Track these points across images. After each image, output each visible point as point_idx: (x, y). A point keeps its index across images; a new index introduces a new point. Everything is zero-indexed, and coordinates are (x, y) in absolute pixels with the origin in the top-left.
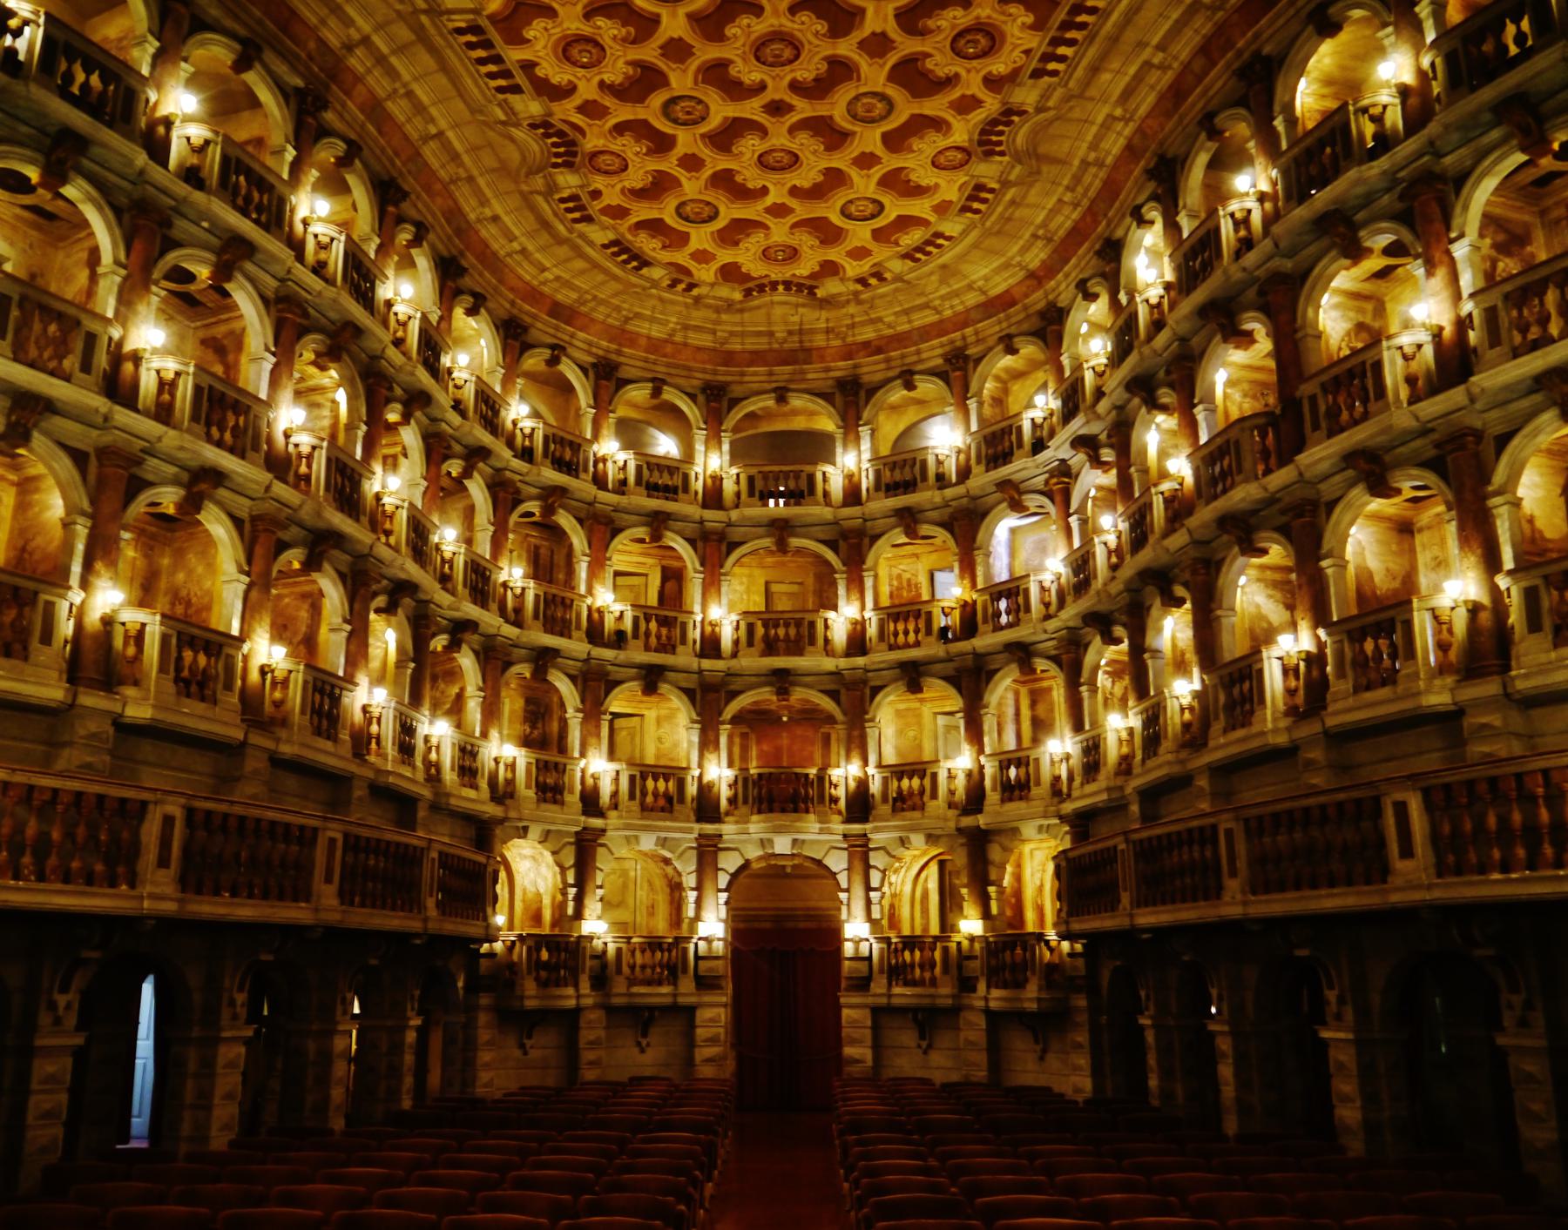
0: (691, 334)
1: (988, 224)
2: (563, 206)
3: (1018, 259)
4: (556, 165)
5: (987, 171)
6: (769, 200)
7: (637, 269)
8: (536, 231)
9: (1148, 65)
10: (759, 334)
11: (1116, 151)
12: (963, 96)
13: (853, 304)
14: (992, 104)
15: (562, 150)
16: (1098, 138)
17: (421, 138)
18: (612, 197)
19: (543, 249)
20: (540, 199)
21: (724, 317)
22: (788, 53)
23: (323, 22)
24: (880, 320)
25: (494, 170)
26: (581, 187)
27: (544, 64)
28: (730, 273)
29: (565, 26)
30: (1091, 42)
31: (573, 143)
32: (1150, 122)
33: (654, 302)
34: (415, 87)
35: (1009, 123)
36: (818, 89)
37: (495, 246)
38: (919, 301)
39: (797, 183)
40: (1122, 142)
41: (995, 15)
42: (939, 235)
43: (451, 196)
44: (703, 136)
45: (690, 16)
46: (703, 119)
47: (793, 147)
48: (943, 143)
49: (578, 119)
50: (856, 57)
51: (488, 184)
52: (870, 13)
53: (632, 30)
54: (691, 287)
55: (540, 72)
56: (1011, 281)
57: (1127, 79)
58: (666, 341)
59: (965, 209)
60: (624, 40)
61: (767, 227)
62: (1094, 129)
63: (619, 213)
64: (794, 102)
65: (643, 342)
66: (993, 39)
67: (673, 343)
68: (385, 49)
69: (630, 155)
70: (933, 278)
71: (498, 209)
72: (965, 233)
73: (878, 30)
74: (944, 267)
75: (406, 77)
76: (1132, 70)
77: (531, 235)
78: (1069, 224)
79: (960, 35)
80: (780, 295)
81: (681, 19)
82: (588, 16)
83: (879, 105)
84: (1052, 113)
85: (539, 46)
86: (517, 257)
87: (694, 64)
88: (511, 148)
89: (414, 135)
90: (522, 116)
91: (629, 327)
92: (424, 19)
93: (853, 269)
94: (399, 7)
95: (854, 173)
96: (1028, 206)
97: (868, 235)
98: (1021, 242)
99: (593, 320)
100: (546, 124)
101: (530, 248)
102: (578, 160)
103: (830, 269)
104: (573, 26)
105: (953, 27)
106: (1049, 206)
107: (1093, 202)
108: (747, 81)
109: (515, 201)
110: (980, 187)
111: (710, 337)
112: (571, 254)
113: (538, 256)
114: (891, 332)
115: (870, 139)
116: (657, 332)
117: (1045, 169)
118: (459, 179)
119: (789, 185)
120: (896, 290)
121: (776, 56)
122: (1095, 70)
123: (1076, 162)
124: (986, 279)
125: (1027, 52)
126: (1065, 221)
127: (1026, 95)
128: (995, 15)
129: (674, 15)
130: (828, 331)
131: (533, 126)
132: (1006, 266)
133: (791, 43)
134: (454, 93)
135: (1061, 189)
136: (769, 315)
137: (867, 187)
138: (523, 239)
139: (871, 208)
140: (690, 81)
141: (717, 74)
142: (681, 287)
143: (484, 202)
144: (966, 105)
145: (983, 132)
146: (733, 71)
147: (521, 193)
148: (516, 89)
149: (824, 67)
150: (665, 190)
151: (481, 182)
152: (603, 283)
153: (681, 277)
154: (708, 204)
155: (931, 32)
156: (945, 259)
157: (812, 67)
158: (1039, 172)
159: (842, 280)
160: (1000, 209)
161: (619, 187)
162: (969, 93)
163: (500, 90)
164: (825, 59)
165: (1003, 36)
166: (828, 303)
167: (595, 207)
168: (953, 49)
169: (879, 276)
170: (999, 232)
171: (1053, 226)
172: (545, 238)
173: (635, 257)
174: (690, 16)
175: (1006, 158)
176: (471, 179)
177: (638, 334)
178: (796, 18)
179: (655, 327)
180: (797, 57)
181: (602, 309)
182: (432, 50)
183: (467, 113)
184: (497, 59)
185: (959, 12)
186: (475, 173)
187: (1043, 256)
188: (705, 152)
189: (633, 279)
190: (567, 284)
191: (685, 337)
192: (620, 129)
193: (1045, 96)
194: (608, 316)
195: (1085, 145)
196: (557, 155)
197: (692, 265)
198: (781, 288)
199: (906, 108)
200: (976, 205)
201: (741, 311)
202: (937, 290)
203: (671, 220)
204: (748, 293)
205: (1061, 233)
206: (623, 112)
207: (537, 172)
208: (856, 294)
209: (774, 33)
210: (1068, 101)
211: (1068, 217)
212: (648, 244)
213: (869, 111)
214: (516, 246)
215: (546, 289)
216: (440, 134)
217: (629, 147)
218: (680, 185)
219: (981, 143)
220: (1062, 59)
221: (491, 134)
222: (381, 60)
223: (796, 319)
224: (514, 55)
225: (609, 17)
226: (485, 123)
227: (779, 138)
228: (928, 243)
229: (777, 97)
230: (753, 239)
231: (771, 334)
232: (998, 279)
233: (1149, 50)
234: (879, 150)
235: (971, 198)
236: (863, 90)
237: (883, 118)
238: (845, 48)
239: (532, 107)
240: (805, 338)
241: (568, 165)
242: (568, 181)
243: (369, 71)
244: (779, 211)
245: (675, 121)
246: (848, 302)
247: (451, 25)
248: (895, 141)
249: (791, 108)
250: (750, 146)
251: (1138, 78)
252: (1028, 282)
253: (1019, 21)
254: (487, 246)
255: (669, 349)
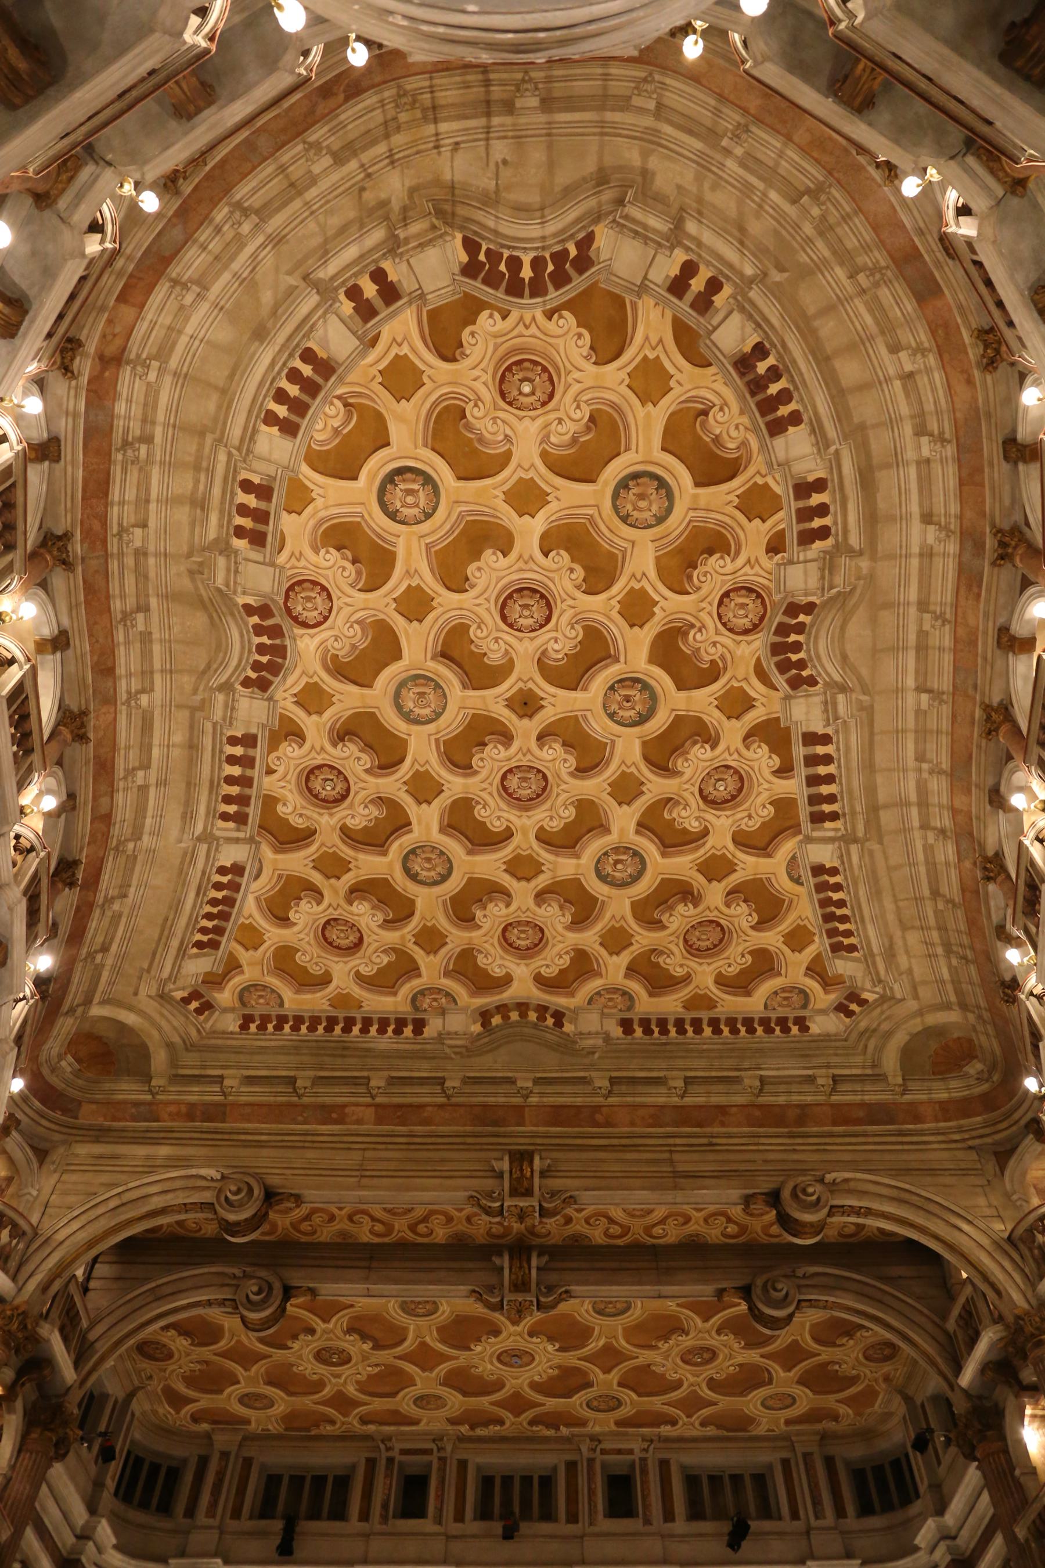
0: (706, 116)
1: (222, 457)
2: (827, 521)
3: (152, 376)
4: (809, 608)
5: (258, 579)
6: (537, 525)
7: (760, 351)
8: (888, 466)
9: (146, 766)
10: (571, 103)
11: (121, 652)
12: (320, 713)
13: (396, 206)
14: (286, 690)
15: (793, 638)
16: (146, 655)
17: (941, 701)
18: (755, 534)
19: (892, 422)
20: (854, 541)
21: (632, 155)
22: (513, 782)
23: (947, 864)
24: (339, 159)
25: (888, 606)
26: (791, 562)
27: (767, 773)
28: (610, 336)
29: (730, 820)
30: (212, 782)
31: (776, 649)
32: (110, 717)
33: (755, 228)
34: (911, 763)
35: (257, 666)
36: (482, 731)
37: (952, 470)
38: (277, 222)
39: (503, 562)
40: (121, 670)
41: (315, 816)
42: (289, 429)
43: (956, 606)
44: (617, 661)
45: (607, 831)
46: (612, 688)
47: (509, 637)
48: (323, 634)
49: (756, 689)
50: (444, 773)
51: (907, 584)
52: (435, 827)
53: (666, 816)
54: (678, 286)
55: (776, 761)
56: (142, 327)
57: (156, 741)
58: (759, 120)
59: (264, 492)
60: (678, 803)
61: (544, 455)
62: (157, 665)
63: (756, 503)
64: (506, 712)
65: (801, 136)
66: (310, 790)
67: (745, 111)
68: (914, 811)
69: (711, 623)
70: (267, 297)
71: (918, 535)
72: (250, 435)
73: (424, 806)
74: (260, 334)
75: (912, 777)
76: (156, 752)
77: (896, 460)
78: (115, 495)
79: (344, 797)
80: (529, 236)
81: (615, 829)
82: (705, 833)
83: (411, 705)
84: (214, 683)
85: (765, 795)
86: (933, 426)
87: (611, 772)
88: (848, 647)
89: (946, 710)
90: (817, 699)
91: (818, 174)
92: (860, 834)
93: (402, 329)
94: (876, 847)
95: (430, 583)
96: (177, 500)
97: (396, 431)
98: (161, 417)
99: (876, 228)
100: (795, 683)
101: (908, 429)
102: (779, 618)
103: (445, 336)
104: (723, 820)
105: (351, 806)
106: (153, 506)
107: (106, 556)
108: (557, 746)
109: (889, 537)
110: (258, 539)
111: (672, 99)
112: (852, 401)
113: (904, 409)
114: (317, 134)
115: (417, 643)
116: (767, 144)
117: (186, 583)
118: (936, 618)
119: (513, 555)
120: (325, 253)
121: (524, 779)
122: (192, 746)
123: (153, 602)
124: (183, 312)
125: (270, 772)
126: (123, 489)
127: (251, 712)
128: (315, 816)
129: (622, 831)
130: (433, 113)
131: (812, 681)
132: (163, 353)
133: (510, 795)
134: (877, 738)
135: (151, 548)
136: (551, 165)
137: (409, 553)
138: (910, 455)
139: (396, 497)
140: (619, 742)
141: (589, 757)
142: (697, 284)
143: (927, 554)
144: (313, 699)
145: (280, 651)
146: (572, 761)
147: (873, 558)
148: (811, 739)
149: (475, 762)
150: (679, 551)
151: (913, 595)
152: (829, 309)
153: (691, 318)
154: (625, 519)
155: (372, 801)
156: (265, 357)
157: (488, 764)
158: (191, 573)
159: (422, 296)
160: (217, 491)
161: (741, 560)
162: (314, 717)
163: (826, 740)
164: (476, 773)
165: (301, 793)
166: (445, 207)
167: (783, 520)
168: (346, 779)
169: (366, 311)
170: (202, 434)
171: (133, 476)
172: (879, 443)
173: (757, 386)
174: (607, 831)
175: (241, 600)
176: (923, 606)
177: (802, 150)
178: (505, 824)
179: (768, 156)
180: (504, 777)
181: (851, 243)
182: (871, 790)
183: (876, 706)
184: (813, 781)
185: (349, 822)
186: (913, 610)
187: (120, 407)
188: (617, 628)
189: (772, 312)
190: (886, 326)
191: (717, 112)
192: (712, 674)
193: (231, 708)
194: (846, 218)
195: (156, 636)
196: (800, 628)
197: (674, 362)
198: (527, 273)
199: (377, 696)
200: (251, 501)
201: (601, 179)
202: (254, 256)
203: (681, 476)
204: (583, 263)
205: (117, 472)
206: (702, 701)
207: (839, 593)
208: (393, 247)
209: (527, 810)
210: (203, 700)
211: (122, 503)
212: (732, 423)
213: (422, 694)
214: (926, 452)
215: (924, 337)
216: (920, 689)
217: (709, 641)
218: (658, 559)
219: (276, 632)
220: (232, 760)
221: (864, 672)
222: (923, 804)
223: (500, 149)
224: (794, 787)
225: (685, 831)
226: (865, 691)
227: (525, 649)
228: (299, 408)
229: (526, 721)
230: (569, 428)
231: (548, 104)
232: (166, 319)
233: (153, 780)
234: (399, 623)
235: (261, 517)
236: (431, 728)
237: (402, 685)
238: (455, 785)
239: (806, 713)
240: (478, 92)
241: (793, 609)
242: (801, 578)
243: (940, 806)
244: (526, 498)
245: (646, 687)
246: (405, 221)
247: (838, 824)
248: (384, 645)
249: (510, 704)
250: (561, 640)
251: (146, 748)
252: (118, 342)
253: (290, 809)
254: (961, 483)
255: (754, 103)
